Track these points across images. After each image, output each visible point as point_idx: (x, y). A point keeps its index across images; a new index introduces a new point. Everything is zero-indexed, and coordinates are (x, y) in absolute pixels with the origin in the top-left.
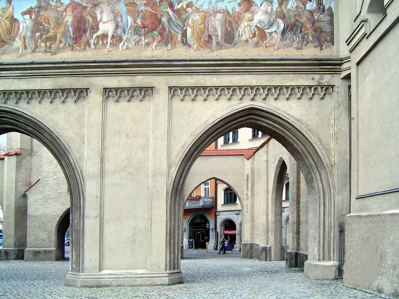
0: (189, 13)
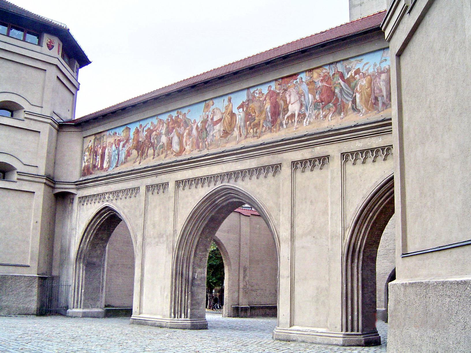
0: (357, 80)
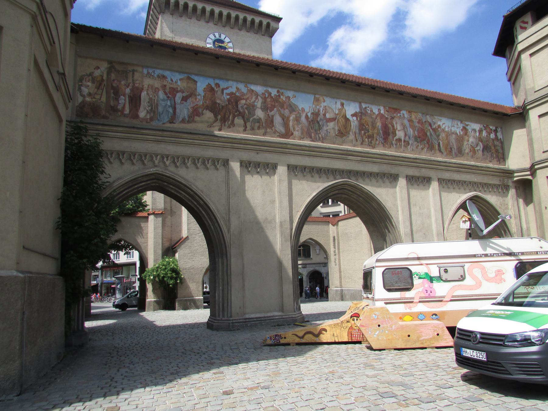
0: (440, 132)
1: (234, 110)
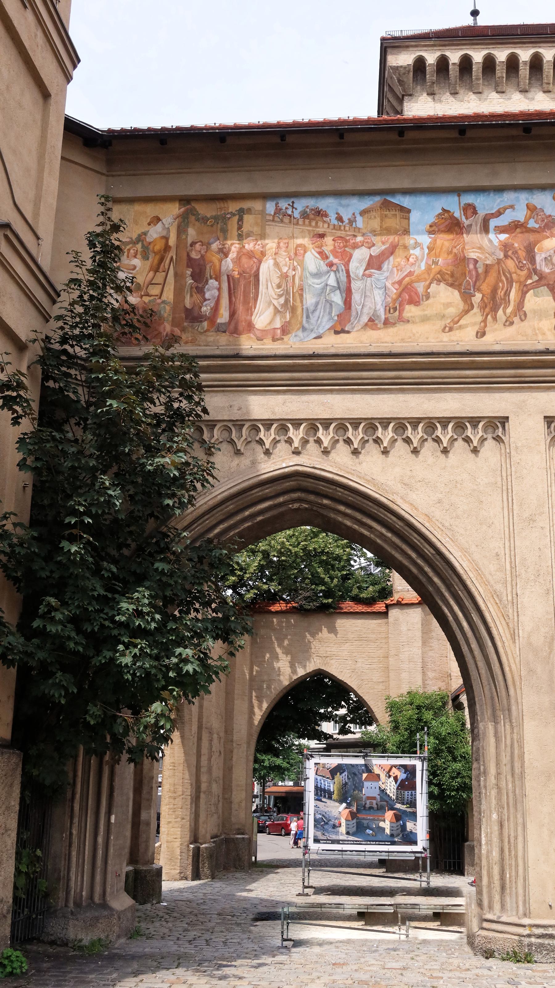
1: (524, 273)
